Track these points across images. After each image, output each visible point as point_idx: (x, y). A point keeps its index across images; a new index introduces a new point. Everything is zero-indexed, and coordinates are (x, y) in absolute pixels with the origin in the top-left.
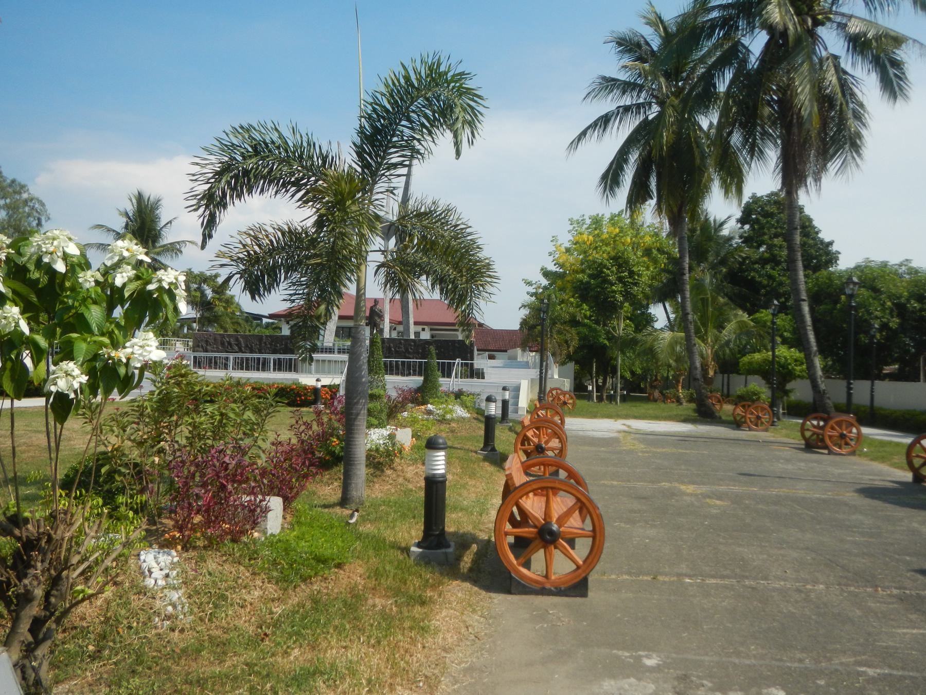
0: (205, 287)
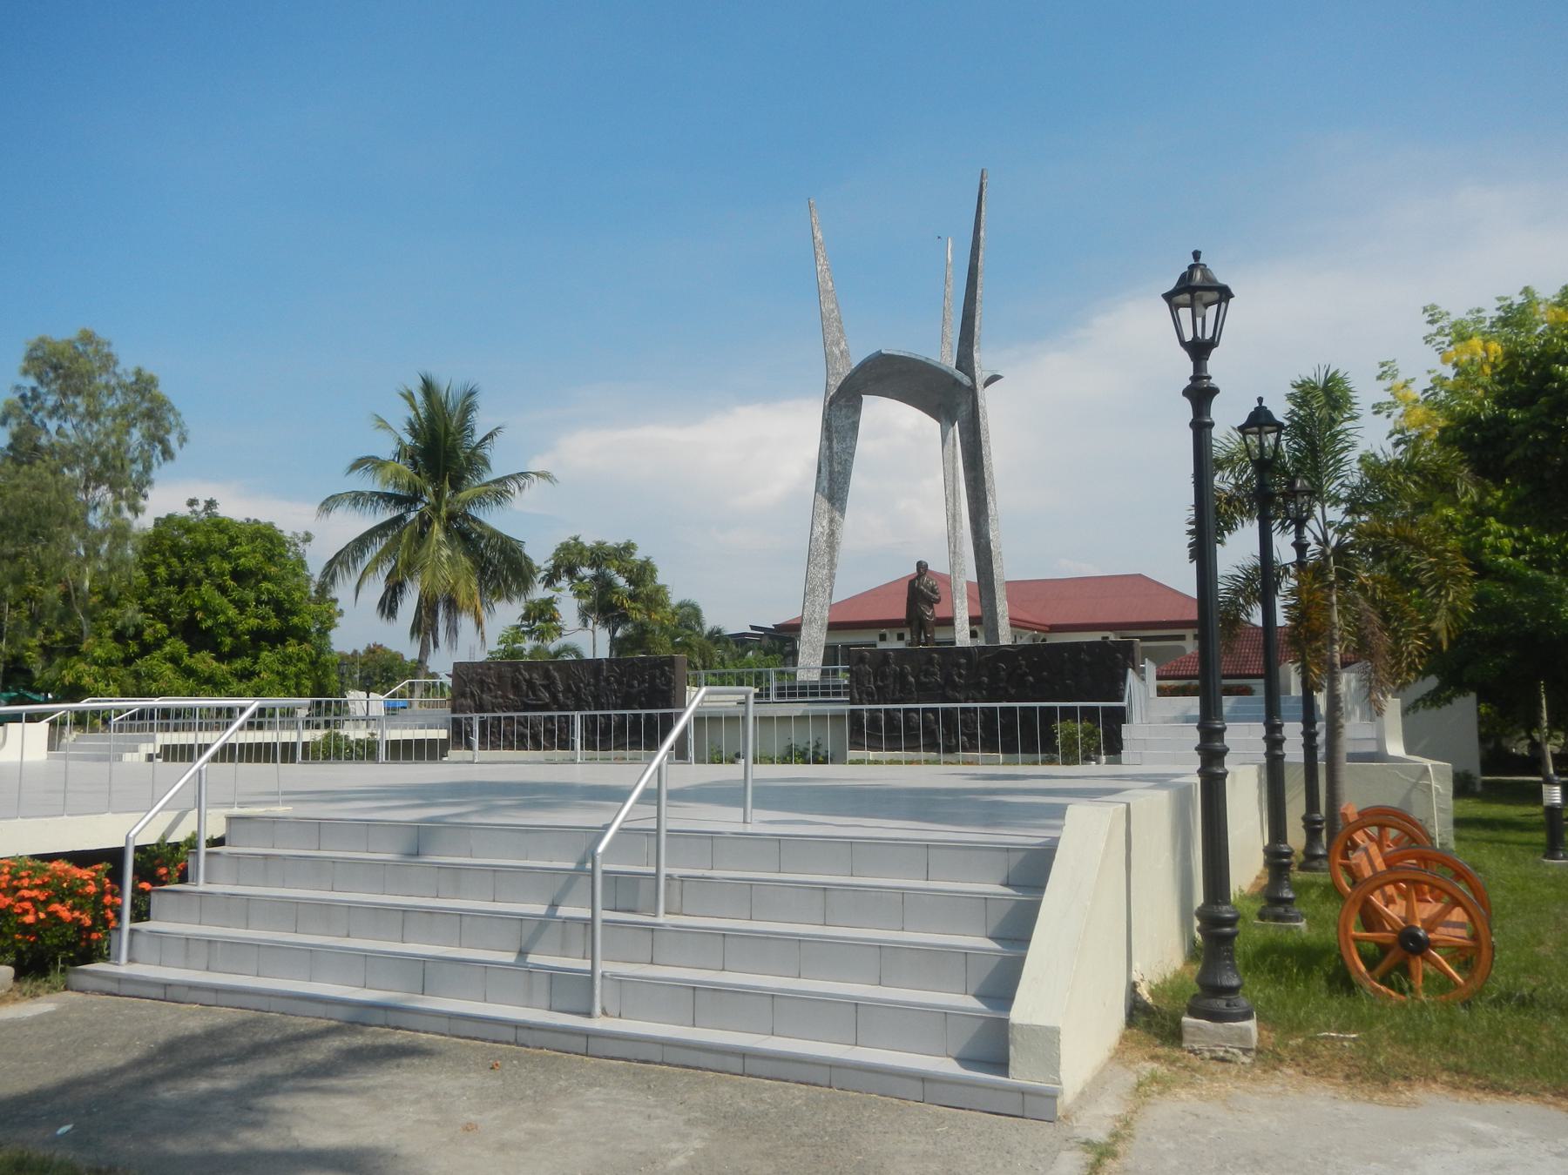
0: (612, 572)
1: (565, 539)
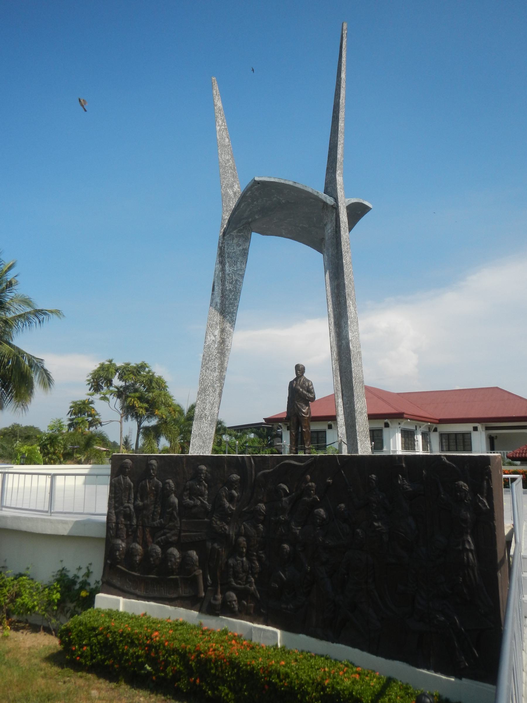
1: (101, 362)
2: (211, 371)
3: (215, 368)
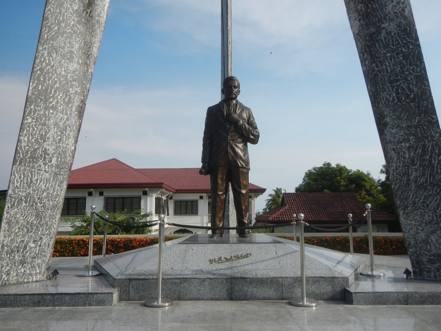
2: (63, 56)
3: (71, 52)
